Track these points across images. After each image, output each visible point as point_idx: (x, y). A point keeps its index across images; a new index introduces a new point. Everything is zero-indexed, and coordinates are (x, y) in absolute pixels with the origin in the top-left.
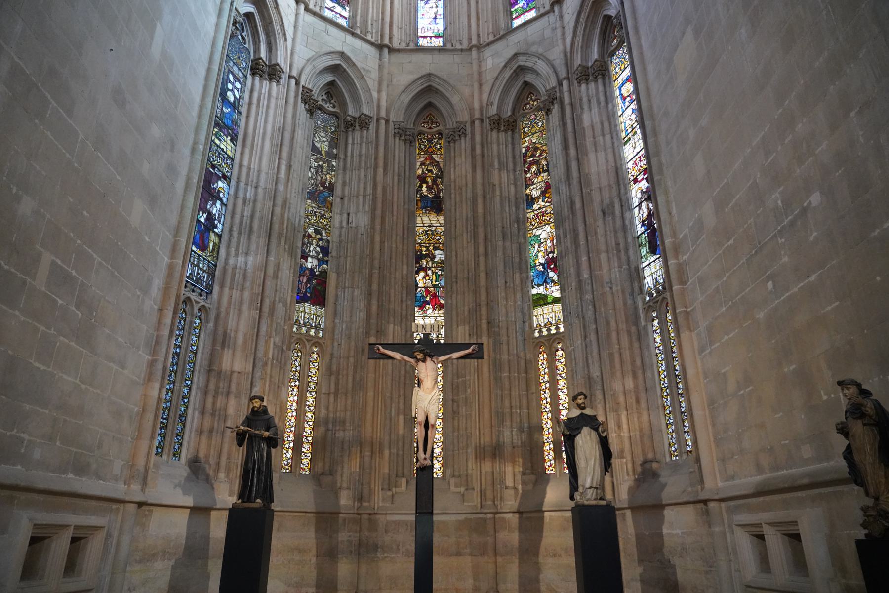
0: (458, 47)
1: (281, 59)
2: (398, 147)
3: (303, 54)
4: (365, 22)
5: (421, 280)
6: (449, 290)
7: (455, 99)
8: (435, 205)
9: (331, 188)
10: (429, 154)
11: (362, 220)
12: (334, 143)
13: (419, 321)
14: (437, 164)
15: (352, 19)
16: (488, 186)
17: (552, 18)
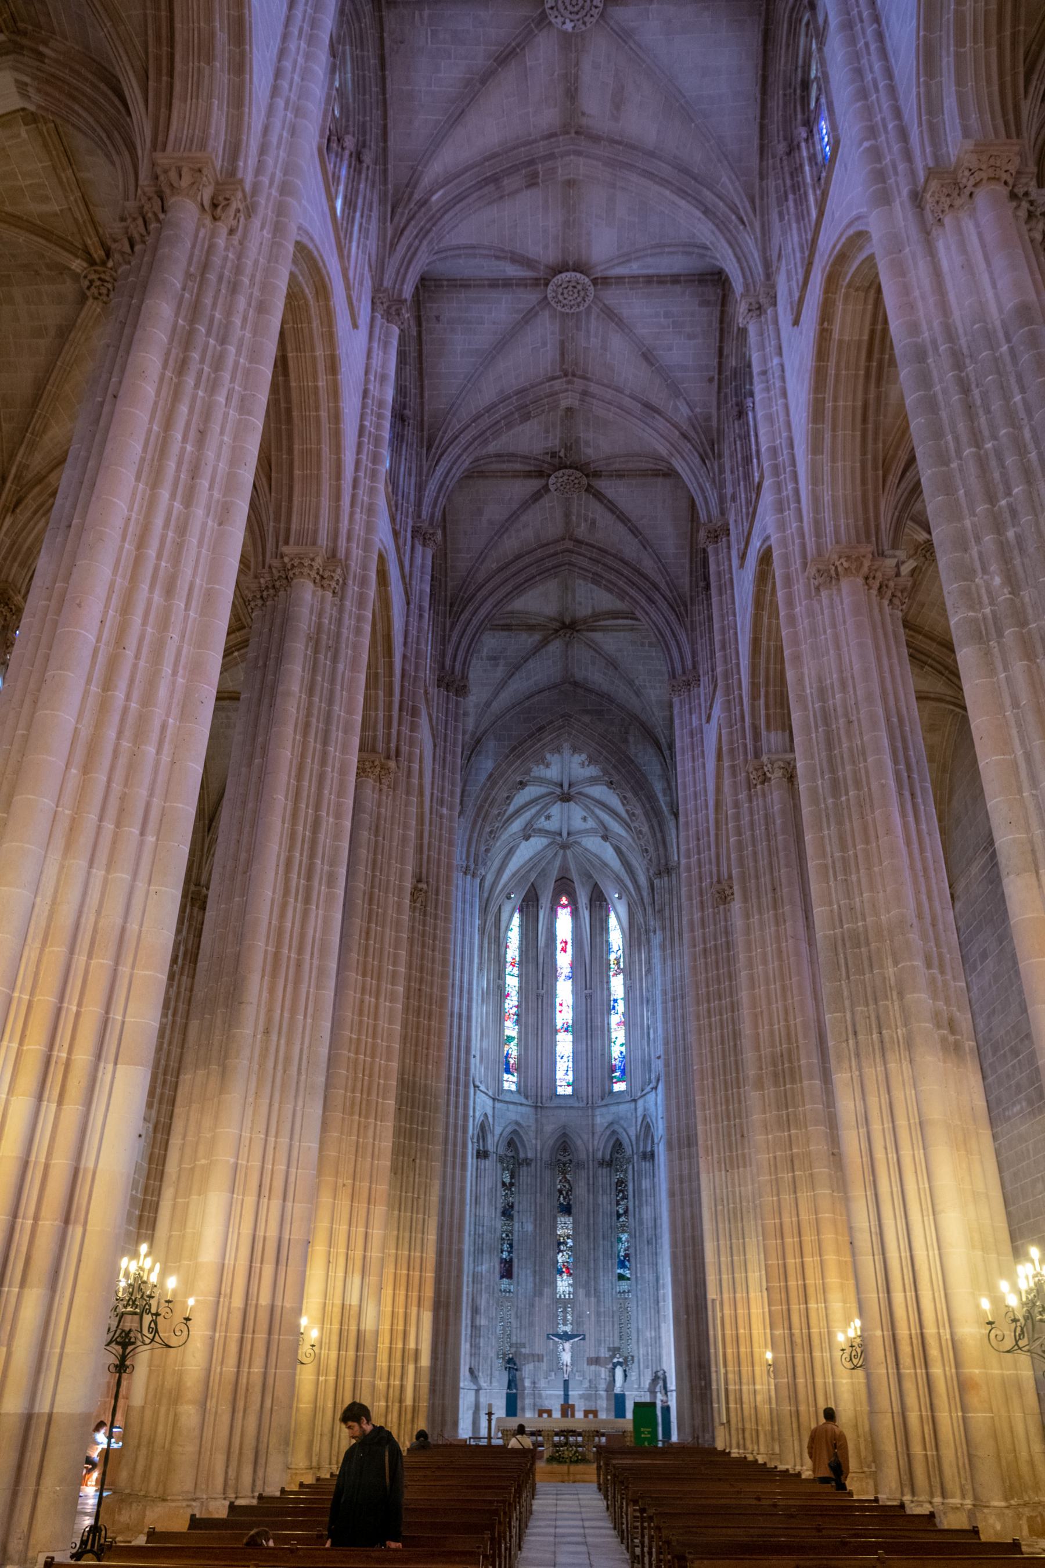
0: (581, 1105)
1: (490, 1148)
2: (547, 1174)
3: (498, 1131)
4: (526, 1086)
5: (560, 1258)
6: (575, 1267)
7: (579, 1142)
8: (567, 1210)
9: (512, 1207)
10: (564, 1172)
11: (529, 1227)
12: (512, 1177)
13: (559, 1283)
14: (568, 1182)
15: (518, 1084)
16: (596, 1205)
17: (633, 1105)
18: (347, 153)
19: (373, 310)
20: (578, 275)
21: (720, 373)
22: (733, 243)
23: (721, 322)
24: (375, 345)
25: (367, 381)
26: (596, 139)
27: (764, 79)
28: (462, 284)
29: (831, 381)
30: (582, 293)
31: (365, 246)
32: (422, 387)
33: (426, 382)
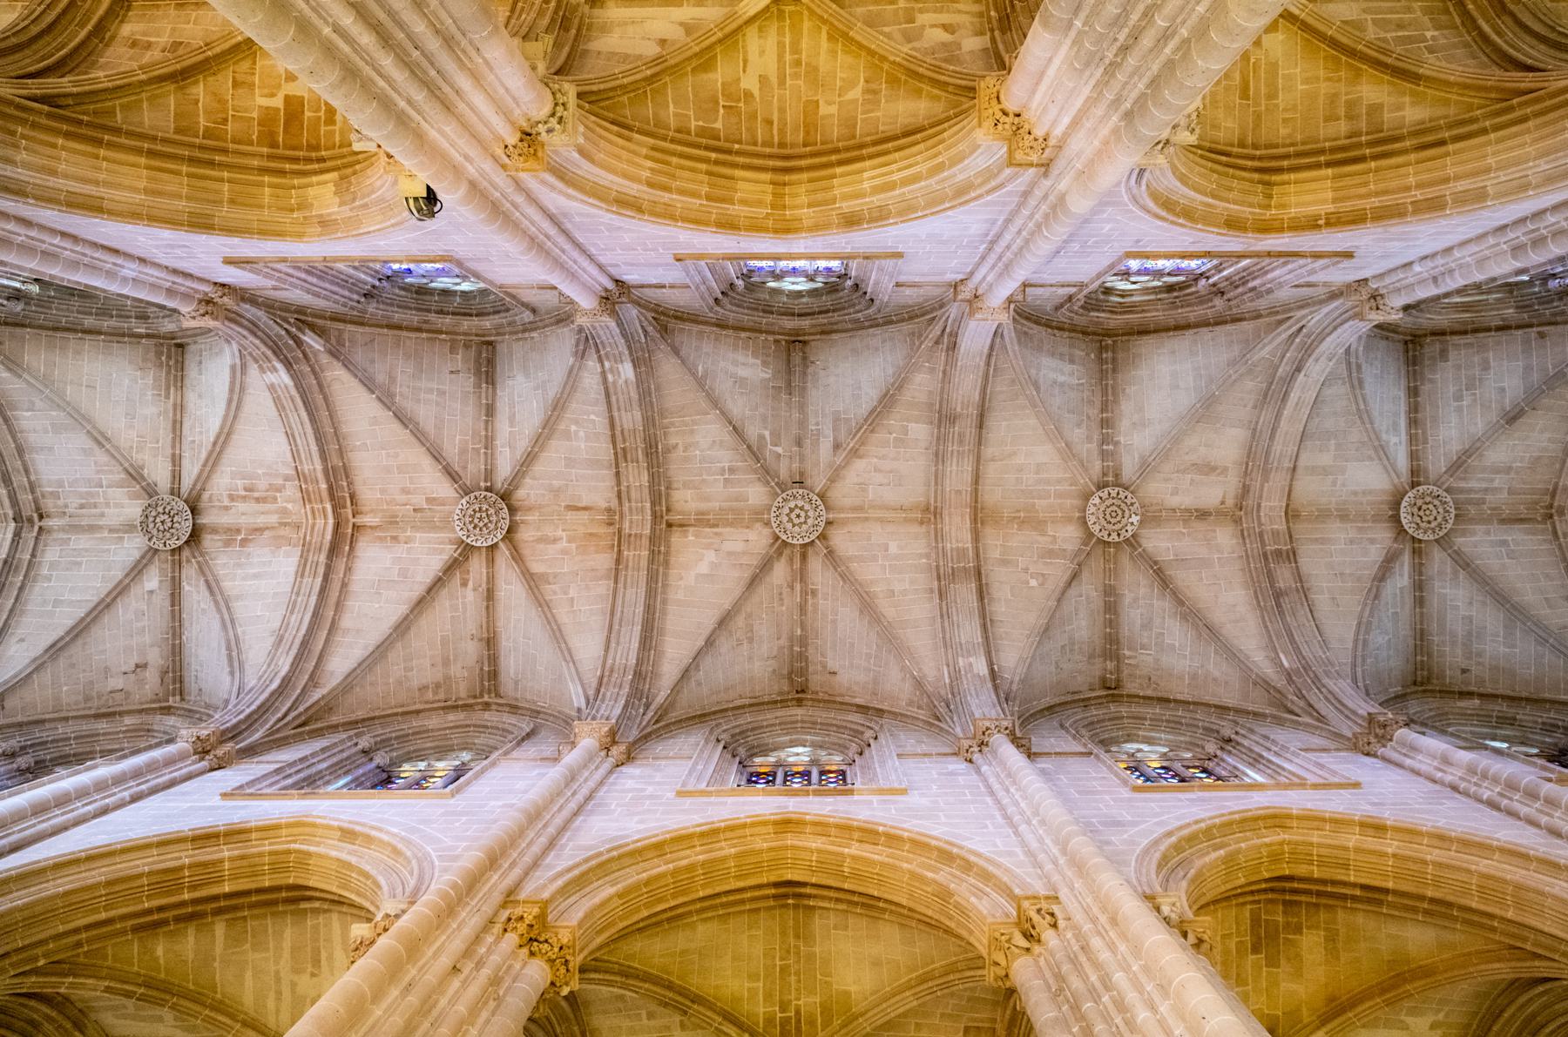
18: (1219, 753)
19: (1375, 756)
20: (1404, 504)
21: (1531, 326)
22: (1322, 337)
23: (1465, 333)
24: (1408, 762)
25: (1442, 783)
26: (1246, 490)
27: (1177, 328)
28: (1421, 638)
29: (1387, 200)
30: (1428, 499)
31: (1293, 753)
32: (1553, 702)
33: (1547, 695)
